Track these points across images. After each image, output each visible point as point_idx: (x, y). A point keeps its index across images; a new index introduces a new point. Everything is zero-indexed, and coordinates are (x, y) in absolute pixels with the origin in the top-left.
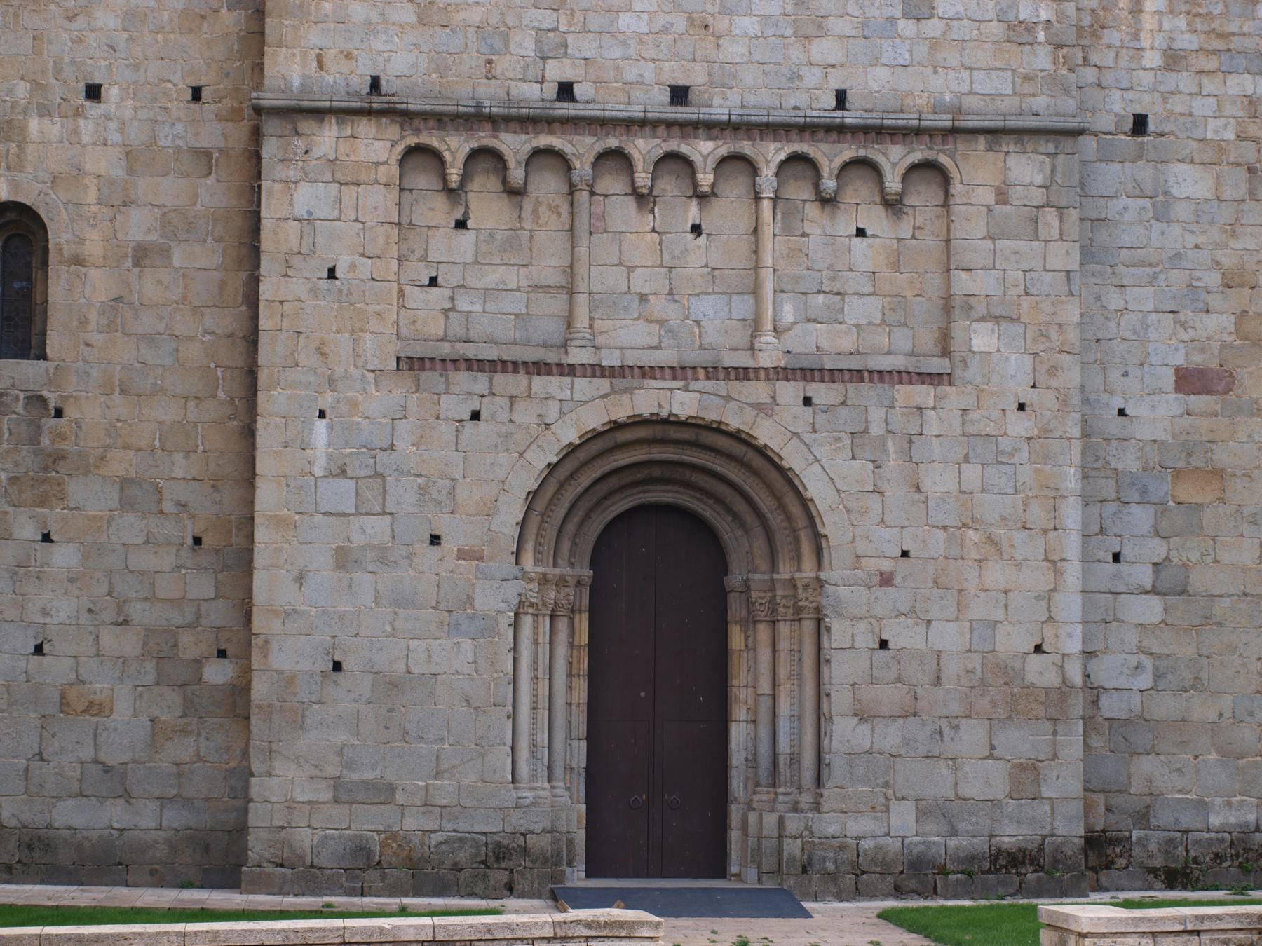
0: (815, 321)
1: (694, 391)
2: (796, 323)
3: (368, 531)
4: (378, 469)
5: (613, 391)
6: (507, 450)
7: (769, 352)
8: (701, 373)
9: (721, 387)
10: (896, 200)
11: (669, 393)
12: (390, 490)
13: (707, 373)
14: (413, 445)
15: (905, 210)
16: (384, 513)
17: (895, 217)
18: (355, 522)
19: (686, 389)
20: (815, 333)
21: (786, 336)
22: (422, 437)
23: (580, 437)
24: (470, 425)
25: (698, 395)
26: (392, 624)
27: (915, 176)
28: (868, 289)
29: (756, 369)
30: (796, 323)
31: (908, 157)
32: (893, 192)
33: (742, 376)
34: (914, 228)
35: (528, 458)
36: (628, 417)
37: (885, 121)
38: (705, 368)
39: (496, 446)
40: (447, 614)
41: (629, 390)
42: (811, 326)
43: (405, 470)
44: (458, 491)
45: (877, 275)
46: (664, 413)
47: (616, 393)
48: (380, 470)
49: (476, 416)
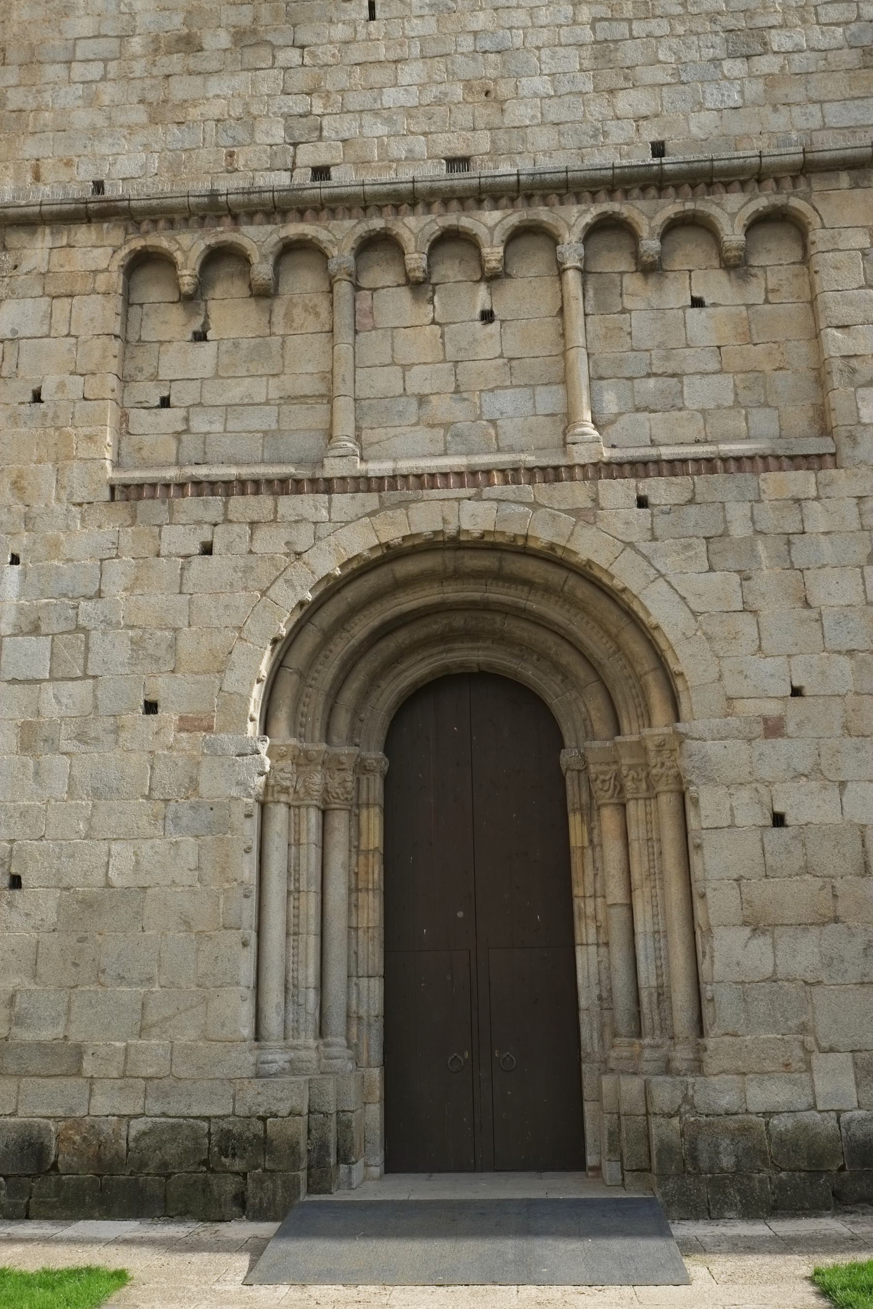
0: (646, 409)
1: (489, 499)
2: (621, 414)
3: (64, 700)
4: (81, 622)
5: (383, 507)
6: (245, 588)
7: (586, 446)
8: (496, 478)
9: (528, 492)
10: (740, 258)
11: (456, 504)
12: (94, 648)
13: (505, 477)
14: (125, 590)
15: (753, 271)
16: (86, 676)
17: (740, 282)
18: (49, 689)
19: (478, 498)
20: (647, 424)
21: (611, 430)
22: (137, 578)
23: (342, 567)
24: (197, 560)
25: (495, 505)
26: (89, 820)
27: (761, 232)
28: (713, 366)
29: (570, 468)
30: (621, 414)
31: (750, 204)
32: (734, 245)
33: (551, 477)
34: (767, 291)
35: (273, 596)
36: (404, 538)
37: (715, 163)
38: (502, 471)
39: (232, 585)
40: (162, 805)
41: (404, 504)
42: (642, 416)
43: (114, 621)
44: (180, 643)
45: (722, 348)
46: (451, 530)
47: (389, 508)
48: (82, 622)
49: (207, 550)
